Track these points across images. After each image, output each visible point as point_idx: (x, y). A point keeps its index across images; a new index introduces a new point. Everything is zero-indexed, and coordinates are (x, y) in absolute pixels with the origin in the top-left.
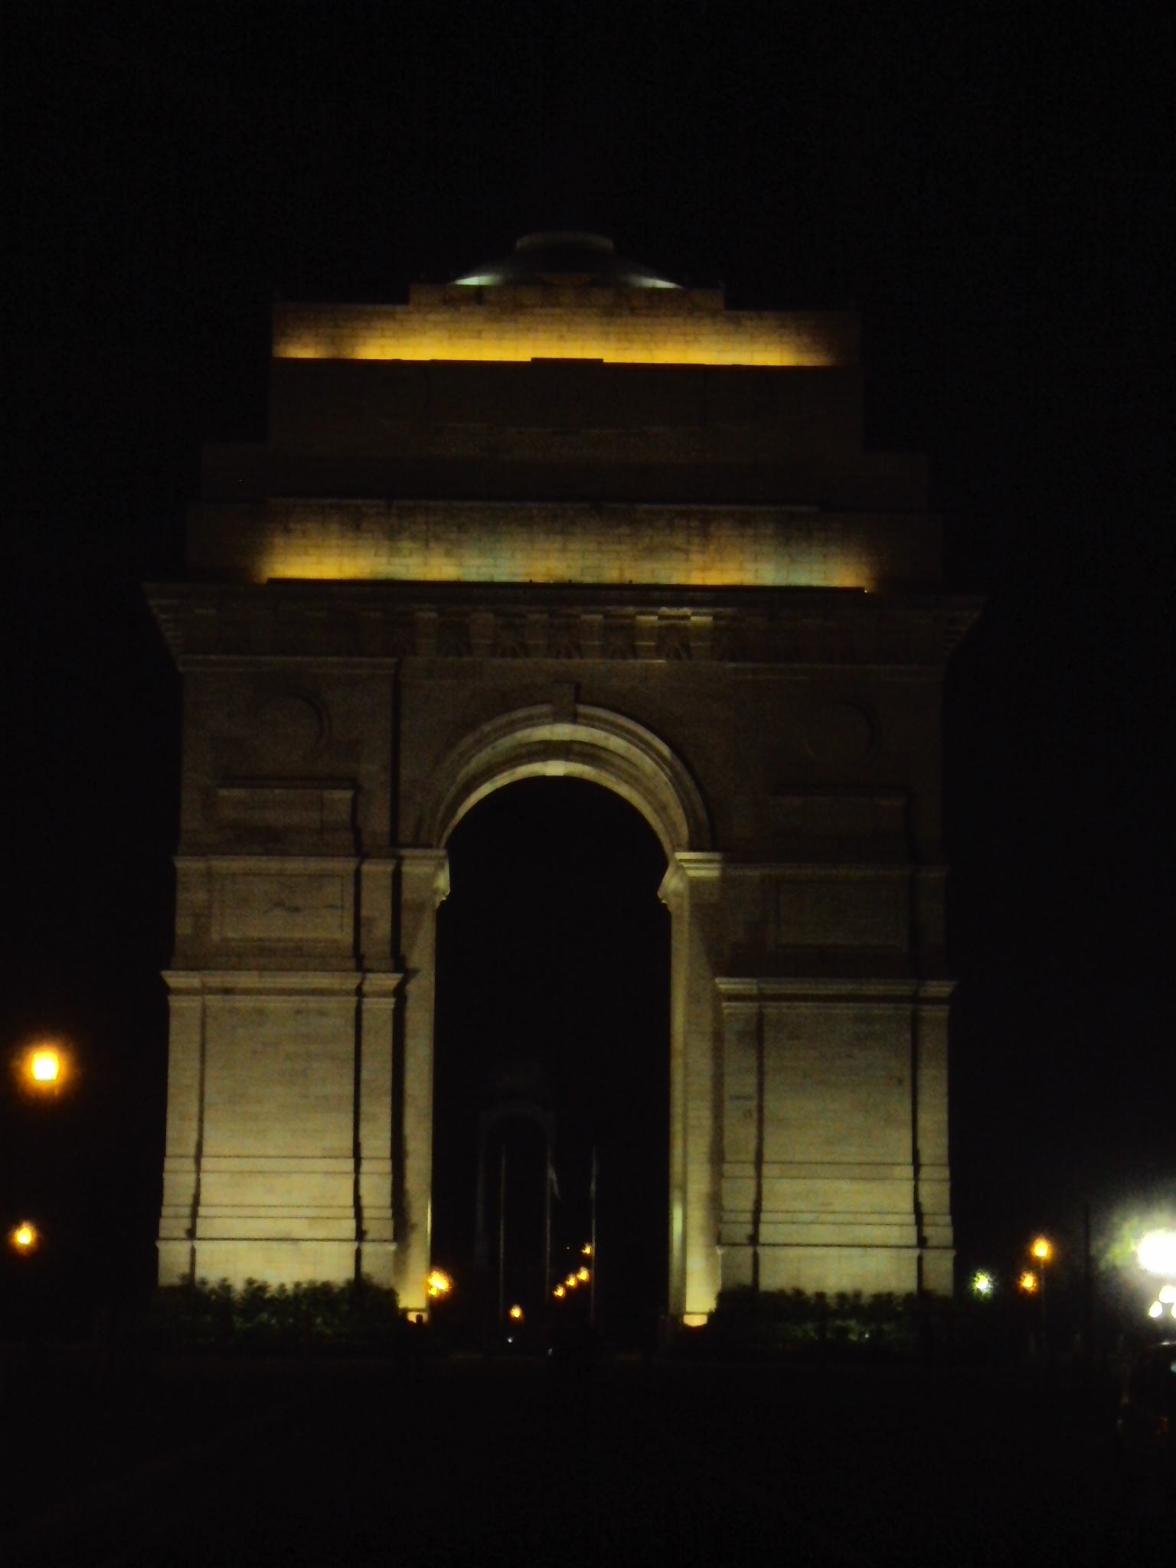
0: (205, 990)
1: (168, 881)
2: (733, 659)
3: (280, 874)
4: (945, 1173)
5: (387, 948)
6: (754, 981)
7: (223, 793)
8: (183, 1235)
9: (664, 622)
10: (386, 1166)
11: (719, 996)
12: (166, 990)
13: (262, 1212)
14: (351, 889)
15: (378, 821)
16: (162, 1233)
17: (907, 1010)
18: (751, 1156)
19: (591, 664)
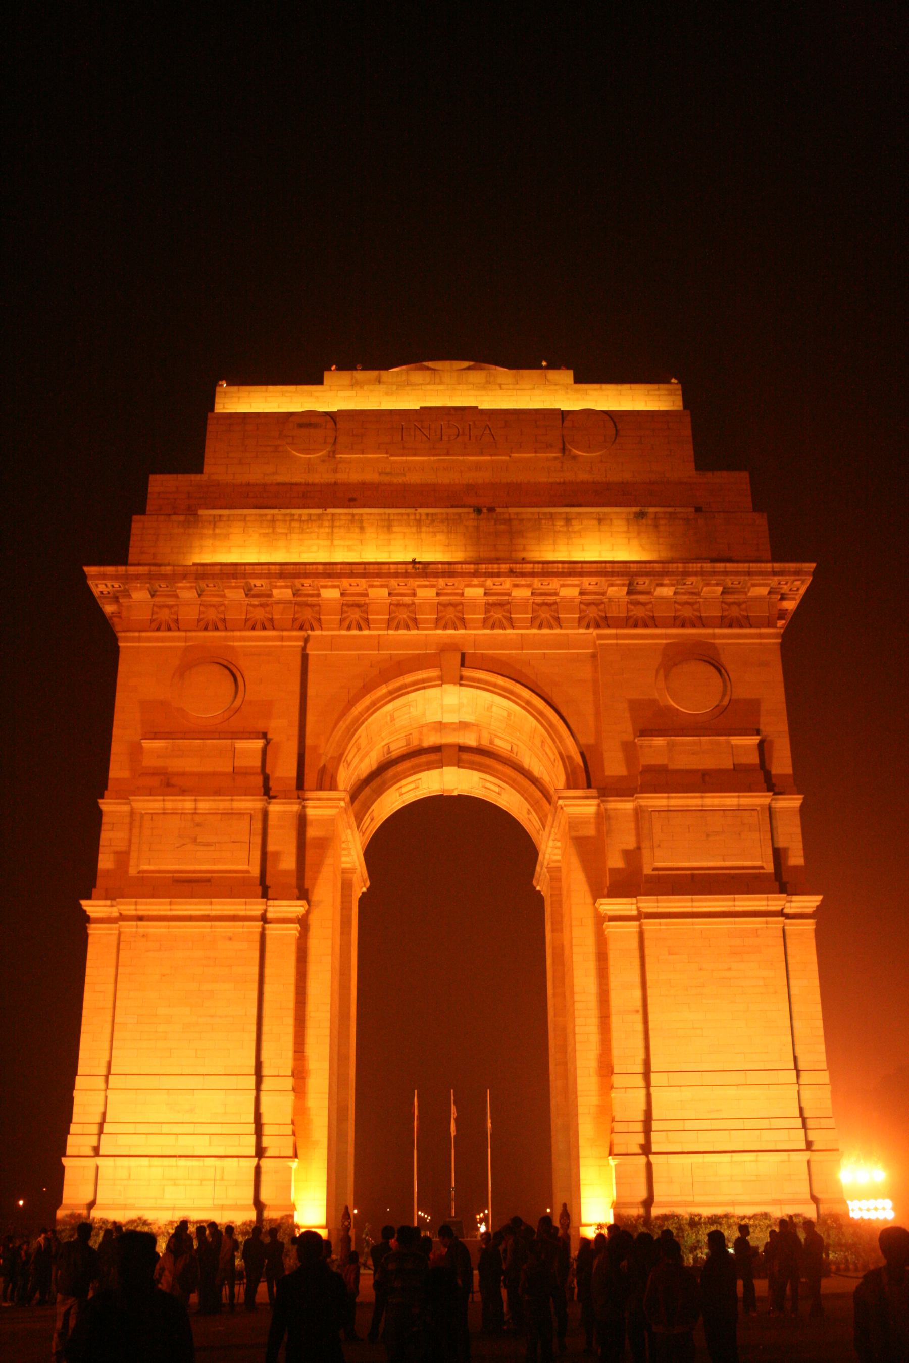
0: (122, 918)
1: (93, 821)
2: (598, 626)
4: (825, 1077)
5: (293, 881)
6: (634, 900)
7: (146, 744)
8: (91, 1153)
9: (539, 599)
10: (289, 1083)
11: (601, 920)
13: (165, 1129)
15: (285, 769)
16: (69, 1152)
18: (640, 1068)
19: (473, 635)
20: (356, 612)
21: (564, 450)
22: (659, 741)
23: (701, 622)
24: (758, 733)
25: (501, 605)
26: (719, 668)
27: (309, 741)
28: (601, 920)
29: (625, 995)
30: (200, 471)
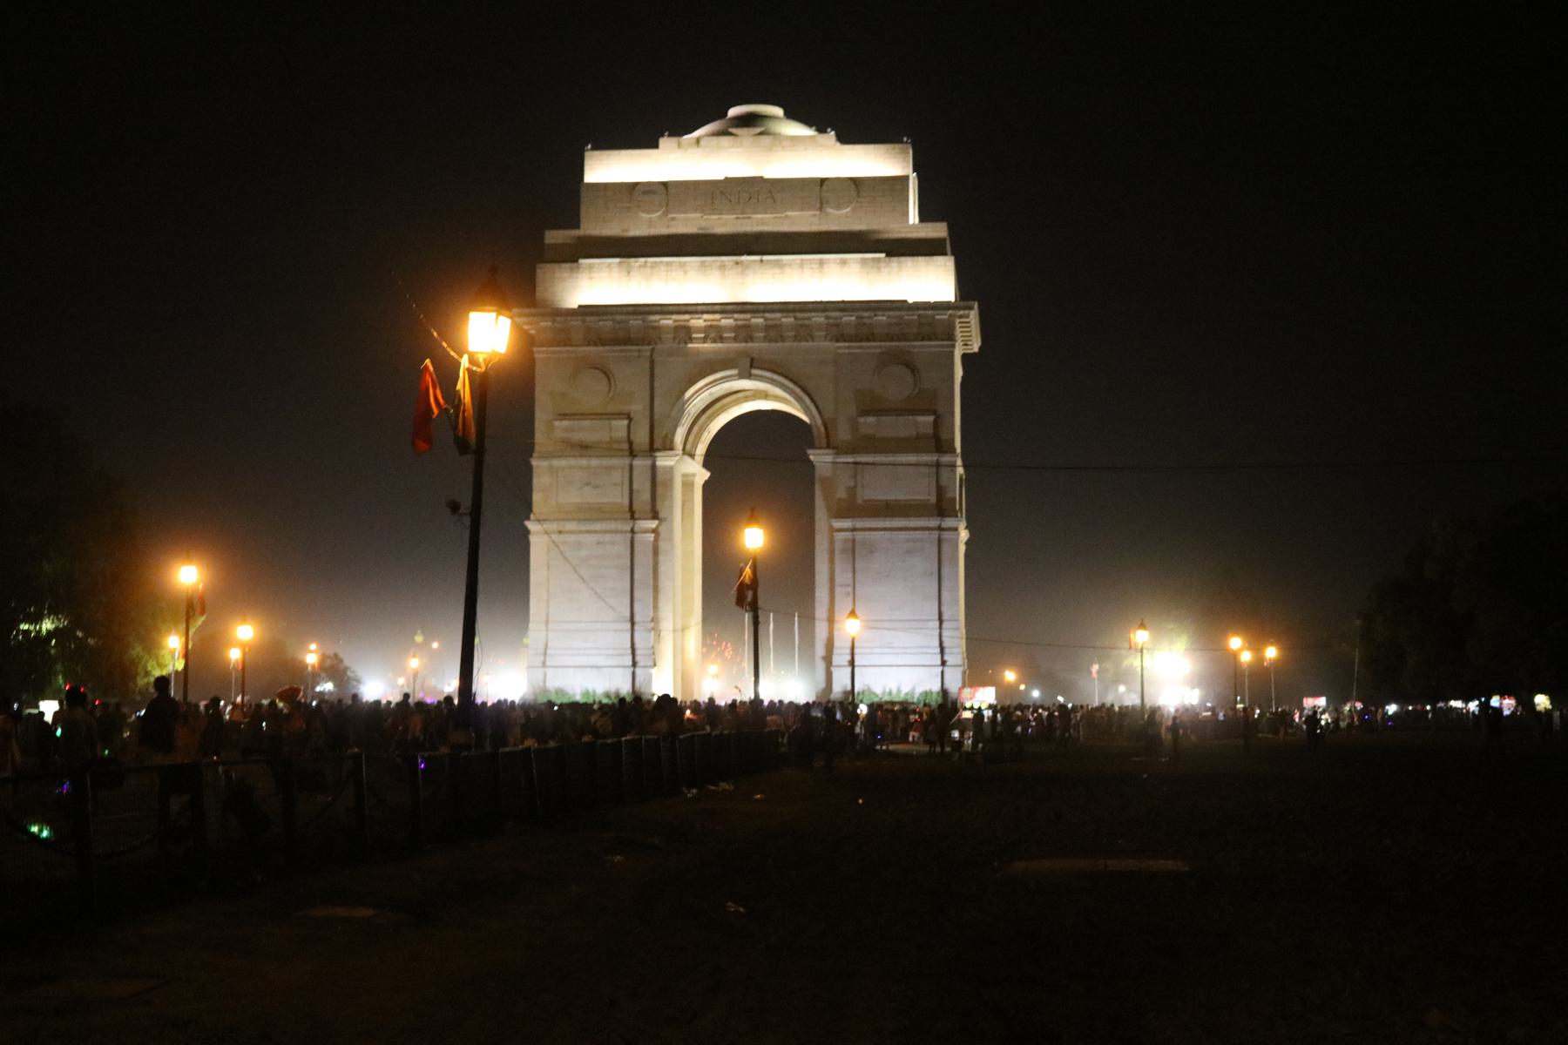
1: (528, 472)
3: (588, 467)
5: (648, 507)
7: (557, 423)
11: (832, 530)
12: (527, 532)
14: (627, 475)
15: (641, 437)
17: (935, 534)
20: (685, 333)
21: (821, 209)
22: (871, 419)
23: (902, 337)
24: (934, 412)
25: (775, 326)
26: (913, 370)
27: (656, 417)
28: (832, 530)
29: (843, 576)
30: (577, 226)
